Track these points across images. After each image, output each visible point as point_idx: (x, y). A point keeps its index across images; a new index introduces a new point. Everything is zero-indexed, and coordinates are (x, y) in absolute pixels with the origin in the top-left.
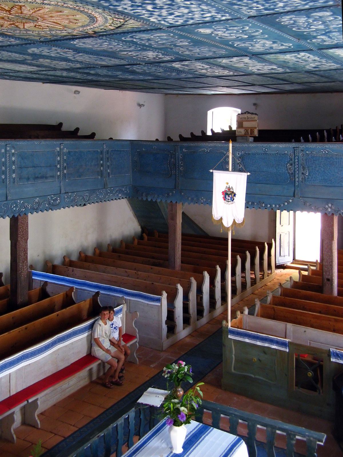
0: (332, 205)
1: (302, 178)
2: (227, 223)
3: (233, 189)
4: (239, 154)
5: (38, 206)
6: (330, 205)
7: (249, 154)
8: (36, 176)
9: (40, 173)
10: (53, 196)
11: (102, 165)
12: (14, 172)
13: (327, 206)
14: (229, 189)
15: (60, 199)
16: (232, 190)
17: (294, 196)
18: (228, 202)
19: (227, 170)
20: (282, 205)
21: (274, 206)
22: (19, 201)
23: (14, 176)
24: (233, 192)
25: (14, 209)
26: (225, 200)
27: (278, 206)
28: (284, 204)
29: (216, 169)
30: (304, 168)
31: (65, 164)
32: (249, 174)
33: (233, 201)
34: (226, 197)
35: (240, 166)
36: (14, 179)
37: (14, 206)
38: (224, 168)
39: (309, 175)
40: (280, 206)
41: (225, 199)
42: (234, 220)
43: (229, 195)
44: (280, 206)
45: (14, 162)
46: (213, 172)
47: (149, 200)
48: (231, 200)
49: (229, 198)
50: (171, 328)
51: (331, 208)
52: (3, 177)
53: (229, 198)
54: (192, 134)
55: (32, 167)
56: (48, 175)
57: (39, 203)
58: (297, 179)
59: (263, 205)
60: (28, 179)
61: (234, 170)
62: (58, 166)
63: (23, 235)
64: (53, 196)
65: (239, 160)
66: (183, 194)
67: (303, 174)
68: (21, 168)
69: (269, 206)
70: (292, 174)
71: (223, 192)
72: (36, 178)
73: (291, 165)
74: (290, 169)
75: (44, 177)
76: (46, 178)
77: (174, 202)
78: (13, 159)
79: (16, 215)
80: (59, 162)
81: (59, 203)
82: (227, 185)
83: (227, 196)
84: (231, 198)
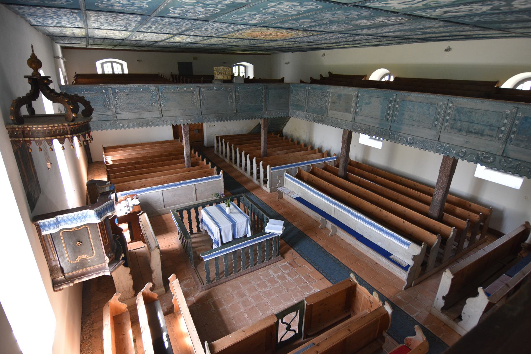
5: (464, 155)
8: (470, 130)
9: (475, 129)
10: (484, 153)
12: (447, 121)
22: (445, 144)
23: (446, 124)
25: (439, 149)
45: (449, 114)
52: (436, 123)
55: (467, 122)
56: (484, 133)
57: (466, 153)
60: (460, 130)
63: (445, 171)
64: (484, 153)
68: (455, 120)
72: (469, 132)
76: (482, 135)
78: (449, 111)
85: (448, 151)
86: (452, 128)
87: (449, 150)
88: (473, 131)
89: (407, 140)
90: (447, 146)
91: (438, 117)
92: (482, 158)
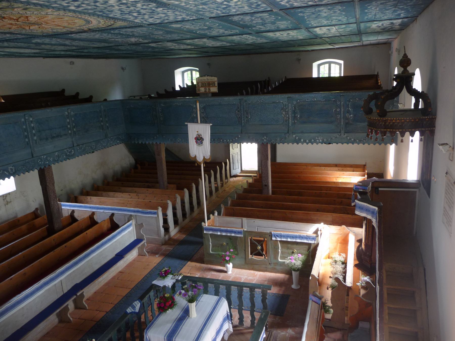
0: (266, 137)
1: (246, 120)
2: (200, 159)
3: (201, 136)
4: (202, 106)
6: (265, 137)
7: (209, 105)
9: (55, 134)
10: (68, 149)
11: (102, 121)
12: (34, 135)
13: (263, 138)
14: (199, 135)
15: (74, 151)
16: (201, 136)
17: (242, 133)
18: (199, 144)
19: (197, 122)
20: (234, 140)
21: (228, 140)
22: (42, 157)
23: (35, 138)
24: (202, 138)
25: (40, 163)
26: (197, 143)
27: (231, 140)
28: (235, 139)
29: (190, 122)
30: (247, 113)
31: (74, 124)
32: (211, 125)
33: (202, 144)
34: (197, 141)
35: (203, 114)
36: (36, 140)
37: (39, 161)
38: (194, 120)
39: (251, 118)
40: (232, 140)
41: (197, 142)
42: (204, 157)
43: (199, 140)
44: (232, 140)
45: (33, 128)
46: (187, 124)
47: (140, 143)
48: (201, 143)
49: (200, 142)
50: (167, 229)
51: (266, 139)
52: (27, 140)
53: (200, 142)
54: (166, 90)
58: (243, 121)
59: (221, 141)
60: (47, 139)
61: (201, 122)
62: (69, 126)
64: (68, 149)
65: (203, 110)
66: (164, 137)
67: (247, 117)
69: (225, 141)
70: (240, 118)
71: (195, 138)
72: (53, 138)
73: (239, 111)
74: (238, 114)
75: (59, 136)
76: (61, 136)
77: (158, 143)
78: (32, 125)
79: (42, 167)
80: (69, 123)
81: (74, 153)
82: (197, 133)
83: (198, 141)
84: (201, 142)
85: (47, 162)
86: (41, 139)
87: (48, 160)
88: (55, 136)
89: (8, 172)
90: (45, 157)
91: (26, 134)
92: (68, 153)
